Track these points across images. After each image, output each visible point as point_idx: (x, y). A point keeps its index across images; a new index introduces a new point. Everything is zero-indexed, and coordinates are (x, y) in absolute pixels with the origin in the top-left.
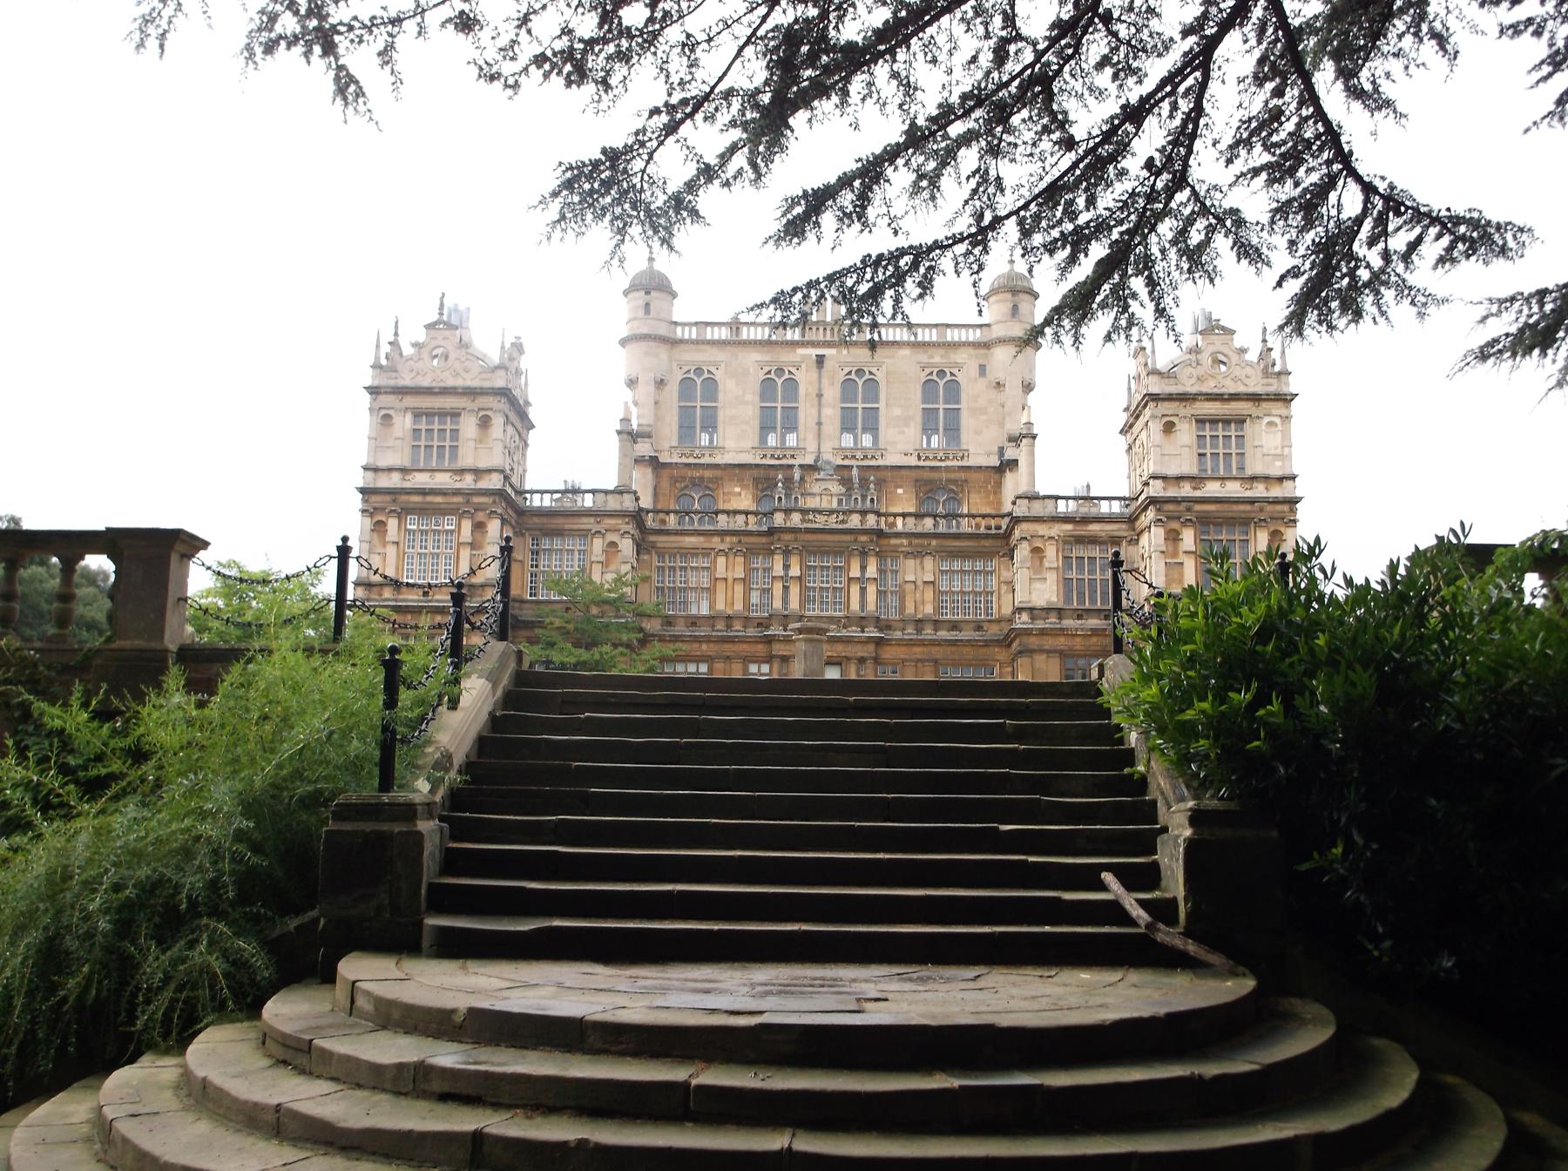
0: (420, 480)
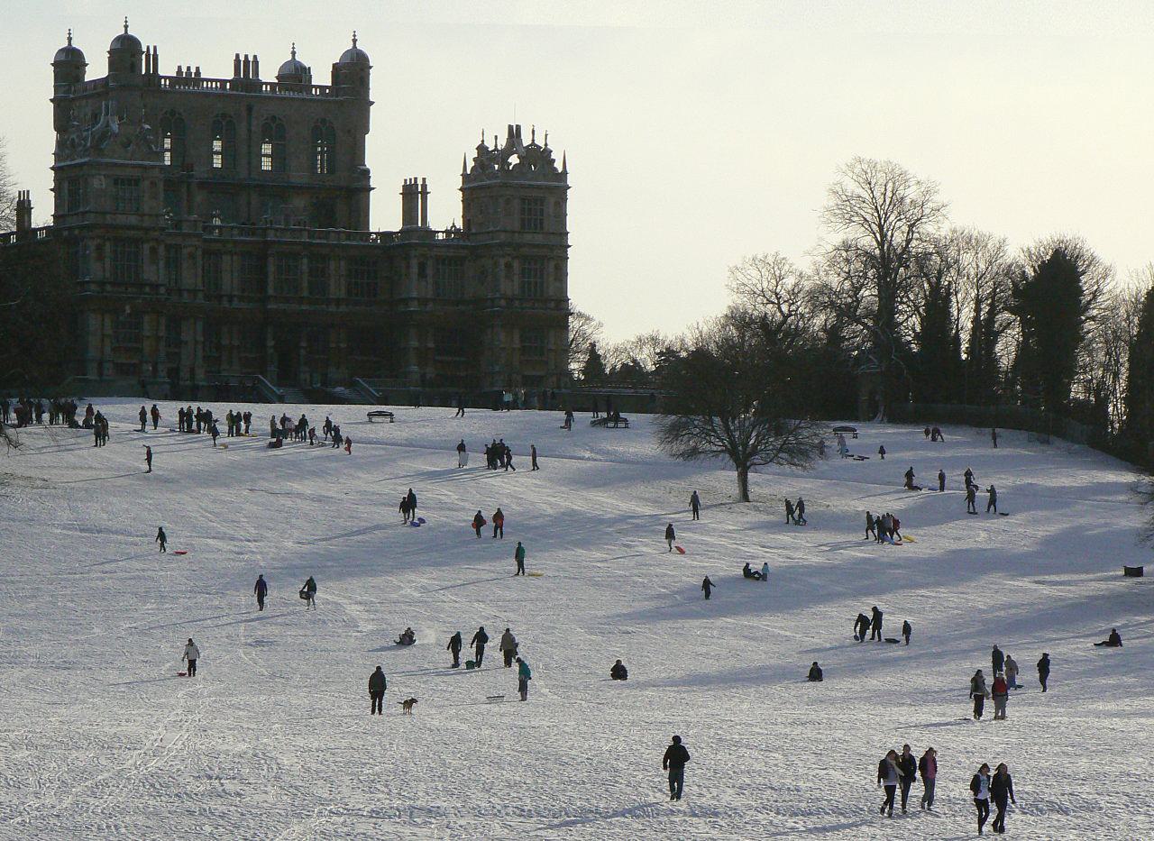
0: (121, 219)
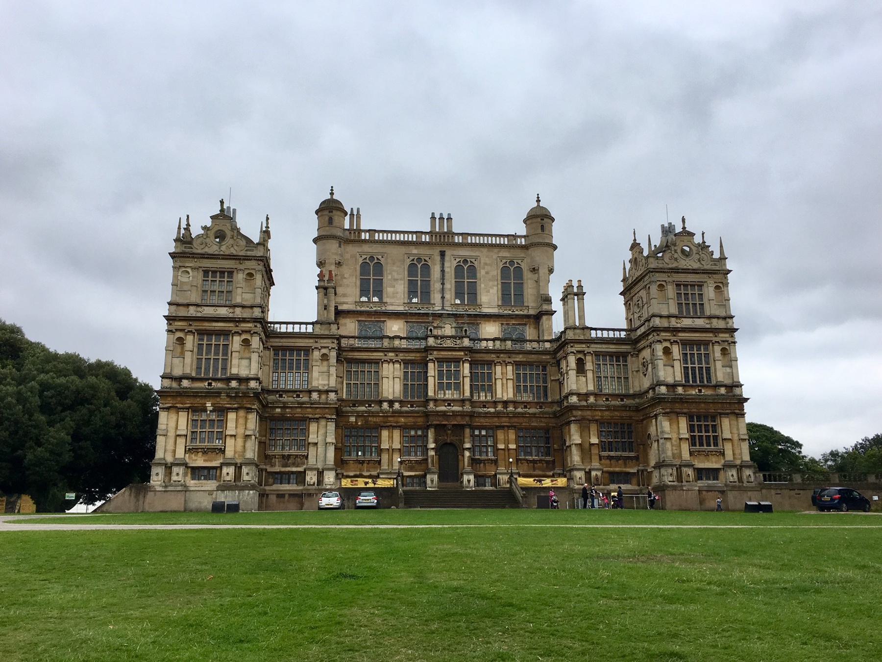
0: (208, 311)
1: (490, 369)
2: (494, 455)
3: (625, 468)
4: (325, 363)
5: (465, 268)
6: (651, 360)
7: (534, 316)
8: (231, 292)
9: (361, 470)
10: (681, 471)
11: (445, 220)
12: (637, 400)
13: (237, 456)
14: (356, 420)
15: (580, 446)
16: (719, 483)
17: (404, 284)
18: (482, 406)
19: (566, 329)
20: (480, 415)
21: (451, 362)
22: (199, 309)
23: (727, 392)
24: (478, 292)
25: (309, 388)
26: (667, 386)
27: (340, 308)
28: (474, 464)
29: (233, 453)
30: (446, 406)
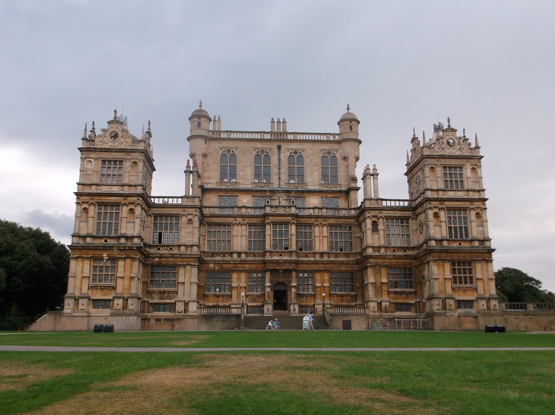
0: (105, 189)
1: (311, 229)
2: (313, 291)
3: (406, 300)
4: (190, 226)
5: (296, 157)
6: (425, 221)
7: (345, 191)
8: (121, 175)
9: (217, 302)
10: (445, 303)
11: (281, 123)
12: (416, 252)
13: (125, 291)
14: (214, 266)
15: (374, 283)
16: (473, 311)
17: (252, 169)
18: (305, 256)
19: (364, 200)
20: (303, 262)
21: (282, 224)
22: (99, 188)
23: (480, 245)
24: (305, 175)
25: (179, 243)
26: (436, 240)
27: (205, 187)
28: (299, 298)
29: (122, 289)
30: (278, 256)
